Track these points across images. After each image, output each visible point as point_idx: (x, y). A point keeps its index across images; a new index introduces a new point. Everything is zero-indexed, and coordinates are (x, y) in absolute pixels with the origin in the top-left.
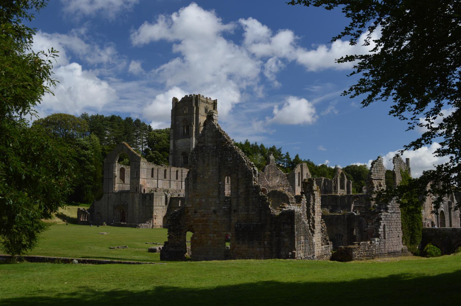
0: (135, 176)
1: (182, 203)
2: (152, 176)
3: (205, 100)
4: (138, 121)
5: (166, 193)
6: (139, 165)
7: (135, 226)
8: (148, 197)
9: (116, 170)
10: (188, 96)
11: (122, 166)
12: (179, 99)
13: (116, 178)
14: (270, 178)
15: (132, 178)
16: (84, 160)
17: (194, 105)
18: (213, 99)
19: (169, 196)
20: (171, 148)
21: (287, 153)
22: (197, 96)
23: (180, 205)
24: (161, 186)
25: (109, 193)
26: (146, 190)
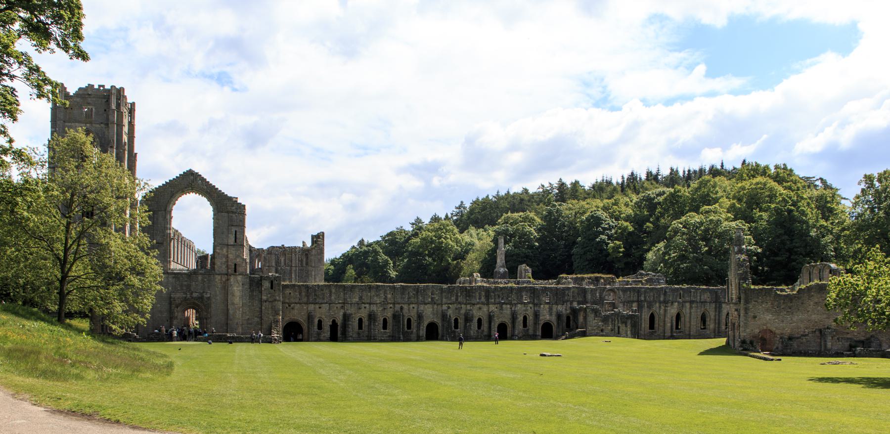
17: (114, 107)
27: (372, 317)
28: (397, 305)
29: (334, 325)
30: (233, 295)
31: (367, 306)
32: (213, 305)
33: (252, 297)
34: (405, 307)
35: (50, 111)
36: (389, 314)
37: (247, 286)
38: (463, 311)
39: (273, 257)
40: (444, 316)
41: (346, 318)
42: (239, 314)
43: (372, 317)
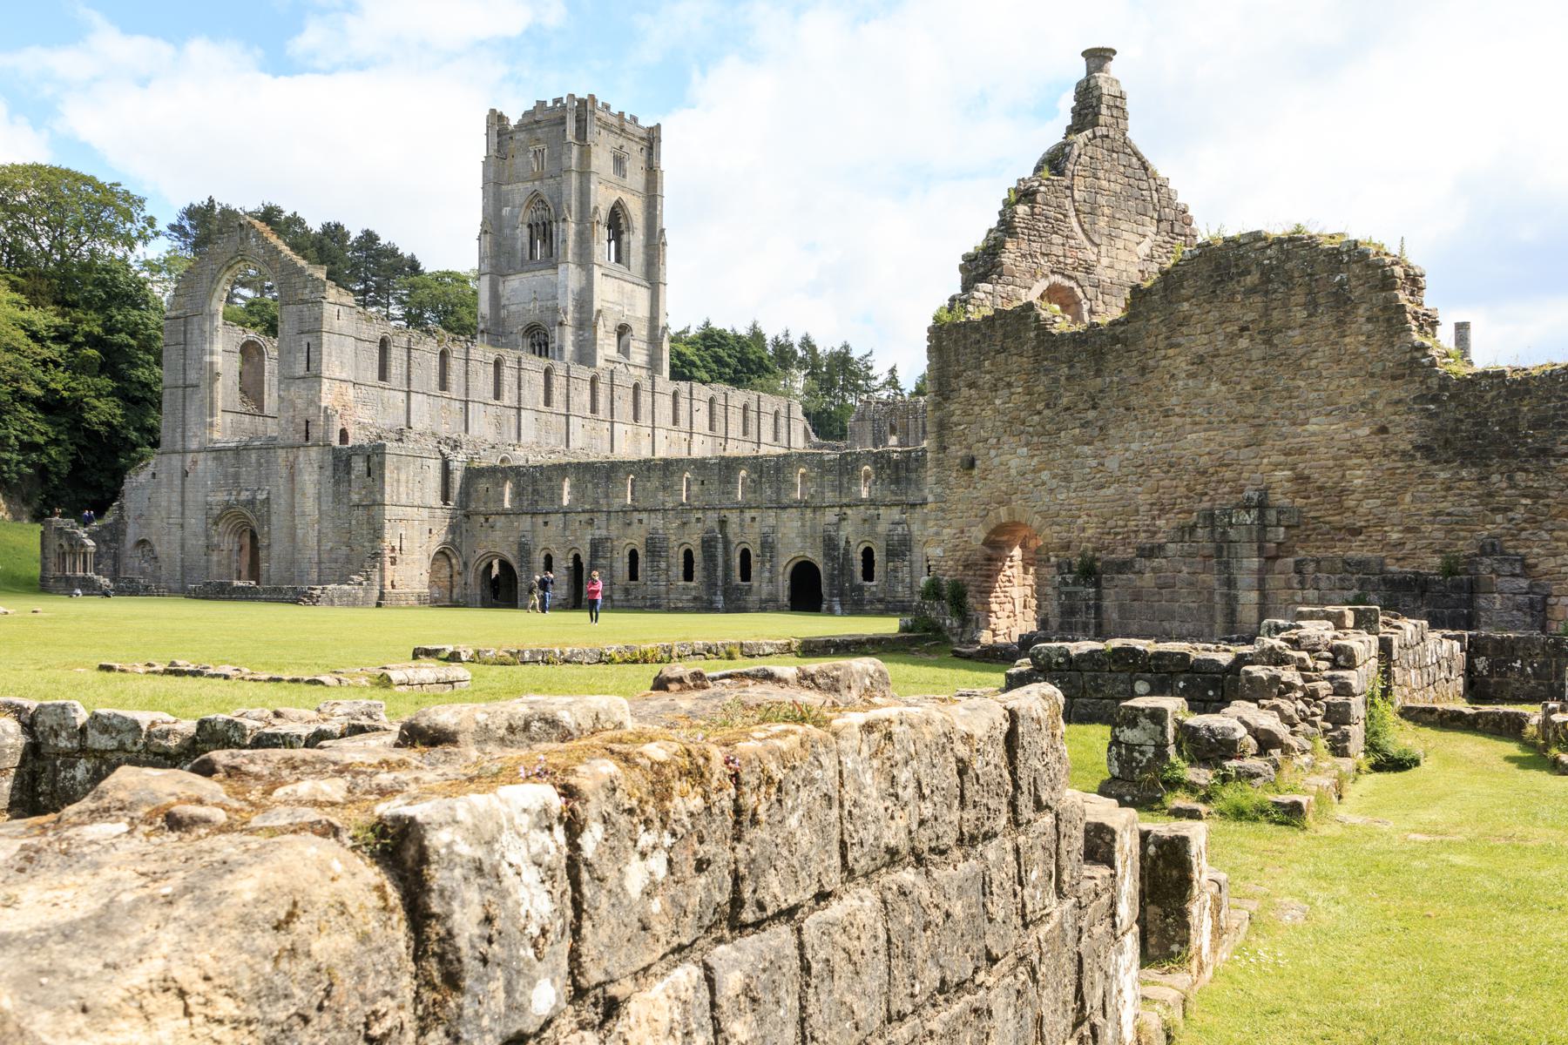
0: (300, 370)
1: (518, 494)
2: (383, 374)
3: (615, 121)
4: (369, 238)
5: (446, 450)
6: (319, 319)
7: (297, 597)
8: (359, 465)
9: (218, 347)
10: (550, 104)
11: (252, 334)
12: (514, 119)
13: (219, 386)
14: (1102, 223)
15: (287, 379)
16: (129, 346)
18: (646, 122)
19: (458, 461)
20: (484, 307)
21: (892, 371)
22: (582, 102)
23: (507, 505)
24: (427, 420)
25: (185, 451)
26: (351, 431)
27: (655, 548)
28: (709, 513)
29: (577, 572)
30: (304, 494)
31: (644, 516)
32: (274, 518)
33: (337, 497)
34: (733, 517)
35: (481, 166)
36: (694, 541)
37: (329, 472)
38: (882, 528)
39: (868, 426)
40: (830, 544)
41: (596, 546)
42: (312, 541)
43: (655, 548)
